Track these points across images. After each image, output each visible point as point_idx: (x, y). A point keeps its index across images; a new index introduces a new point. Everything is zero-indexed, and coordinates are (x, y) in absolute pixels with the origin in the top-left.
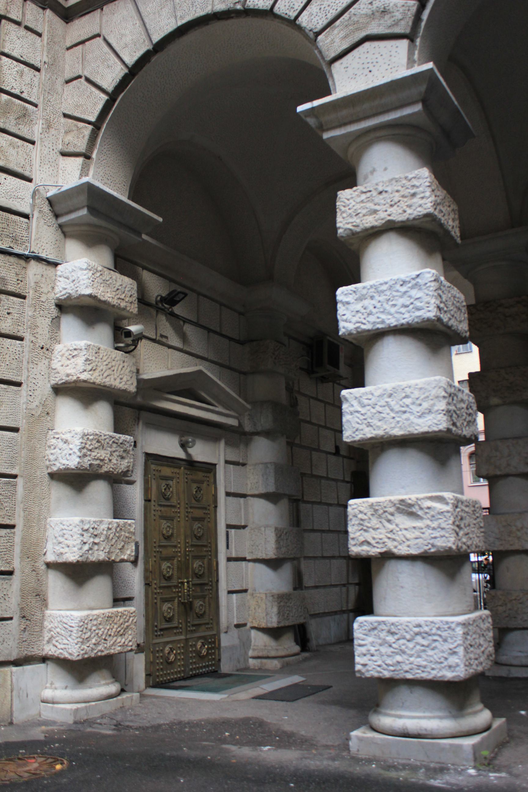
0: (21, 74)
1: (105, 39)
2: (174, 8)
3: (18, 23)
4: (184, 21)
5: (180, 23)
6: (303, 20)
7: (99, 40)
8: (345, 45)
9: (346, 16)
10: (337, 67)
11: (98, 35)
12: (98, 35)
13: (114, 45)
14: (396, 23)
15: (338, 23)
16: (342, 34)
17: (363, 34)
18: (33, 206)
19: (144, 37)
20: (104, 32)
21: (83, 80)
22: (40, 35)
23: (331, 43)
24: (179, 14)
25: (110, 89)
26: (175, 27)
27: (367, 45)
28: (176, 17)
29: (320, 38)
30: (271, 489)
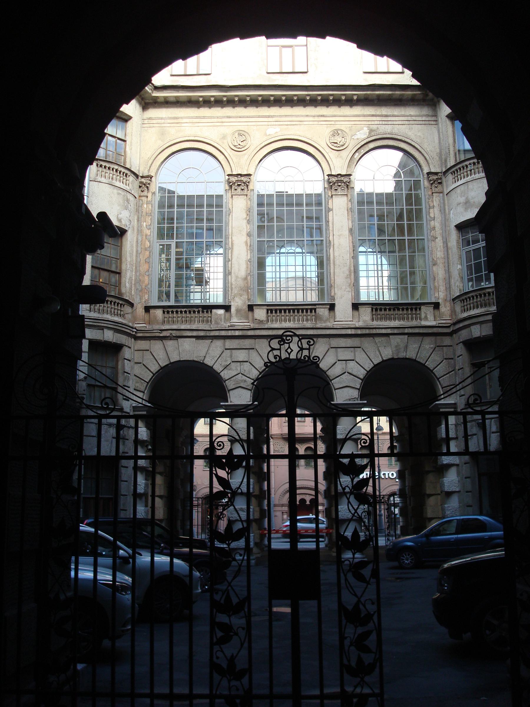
3: (127, 346)
6: (222, 374)
7: (148, 352)
8: (234, 387)
9: (234, 378)
10: (231, 392)
14: (248, 386)
15: (232, 379)
16: (233, 383)
17: (239, 385)
18: (130, 410)
19: (167, 359)
21: (142, 364)
22: (130, 348)
23: (230, 385)
25: (154, 372)
27: (240, 389)
29: (227, 382)
30: (162, 494)
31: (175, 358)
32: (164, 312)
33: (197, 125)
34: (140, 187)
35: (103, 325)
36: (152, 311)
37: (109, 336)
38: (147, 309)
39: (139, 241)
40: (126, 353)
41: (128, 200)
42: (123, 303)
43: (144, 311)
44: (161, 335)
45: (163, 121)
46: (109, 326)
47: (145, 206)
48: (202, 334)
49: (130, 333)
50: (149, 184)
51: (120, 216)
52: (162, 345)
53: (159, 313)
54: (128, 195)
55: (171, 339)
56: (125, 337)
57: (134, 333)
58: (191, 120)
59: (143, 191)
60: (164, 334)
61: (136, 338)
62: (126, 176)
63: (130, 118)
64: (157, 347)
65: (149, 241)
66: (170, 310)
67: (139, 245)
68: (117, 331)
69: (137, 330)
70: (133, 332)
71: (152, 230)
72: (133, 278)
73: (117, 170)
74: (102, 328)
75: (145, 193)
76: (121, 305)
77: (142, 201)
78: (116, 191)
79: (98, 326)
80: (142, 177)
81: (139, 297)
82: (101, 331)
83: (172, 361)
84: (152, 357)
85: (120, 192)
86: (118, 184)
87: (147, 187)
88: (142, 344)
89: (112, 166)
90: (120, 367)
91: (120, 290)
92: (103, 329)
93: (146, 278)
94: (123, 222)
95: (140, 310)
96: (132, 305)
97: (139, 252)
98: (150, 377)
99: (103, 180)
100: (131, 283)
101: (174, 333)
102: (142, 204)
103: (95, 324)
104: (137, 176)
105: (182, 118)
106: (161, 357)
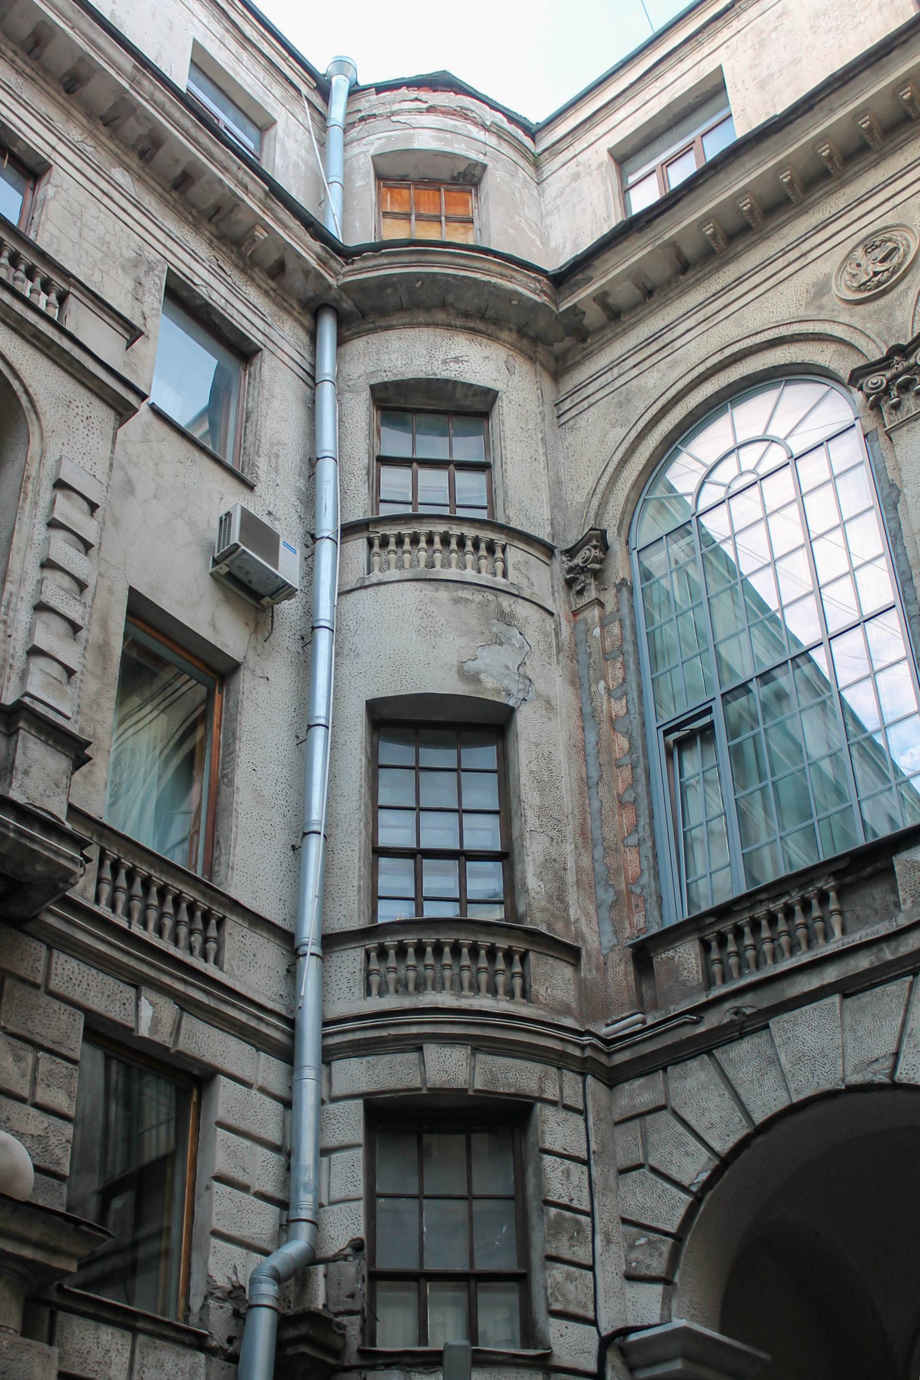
0: (567, 1174)
1: (675, 1113)
2: (783, 1075)
4: (802, 1097)
5: (795, 1099)
7: (664, 1115)
11: (663, 1108)
12: (663, 1108)
13: (693, 1123)
20: (673, 1104)
24: (792, 1086)
26: (787, 1103)
28: (787, 1089)
31: (767, 1101)
32: (706, 947)
33: (722, 315)
34: (569, 583)
35: (414, 1030)
36: (661, 958)
37: (448, 1067)
38: (643, 954)
39: (590, 748)
40: (556, 1130)
41: (506, 618)
42: (519, 946)
43: (631, 968)
44: (701, 1029)
45: (616, 371)
46: (446, 1030)
47: (597, 631)
48: (863, 962)
49: (563, 1054)
50: (601, 561)
51: (471, 666)
52: (712, 1070)
53: (687, 956)
54: (506, 602)
55: (742, 1036)
56: (538, 1068)
57: (588, 1052)
58: (700, 316)
59: (580, 593)
60: (713, 1020)
61: (613, 1078)
62: (491, 549)
63: (489, 396)
64: (696, 1088)
65: (629, 735)
66: (726, 926)
67: (591, 760)
68: (479, 1045)
69: (608, 1042)
70: (583, 1047)
71: (634, 694)
72: (570, 864)
73: (445, 540)
74: (416, 1045)
75: (592, 593)
76: (509, 955)
77: (585, 621)
78: (443, 594)
79: (398, 1038)
80: (571, 553)
81: (608, 927)
82: (414, 1056)
83: (759, 1117)
84: (680, 1128)
85: (465, 594)
86: (452, 573)
87: (597, 575)
88: (638, 1093)
89: (423, 529)
90: (531, 1190)
91: (512, 912)
92: (420, 1049)
93: (631, 857)
94: (489, 682)
95: (621, 972)
96: (571, 954)
97: (595, 779)
98: (681, 1212)
99: (393, 574)
100: (560, 880)
101: (750, 1003)
102: (588, 631)
103: (383, 1033)
104: (548, 550)
105: (669, 327)
106: (715, 1116)
